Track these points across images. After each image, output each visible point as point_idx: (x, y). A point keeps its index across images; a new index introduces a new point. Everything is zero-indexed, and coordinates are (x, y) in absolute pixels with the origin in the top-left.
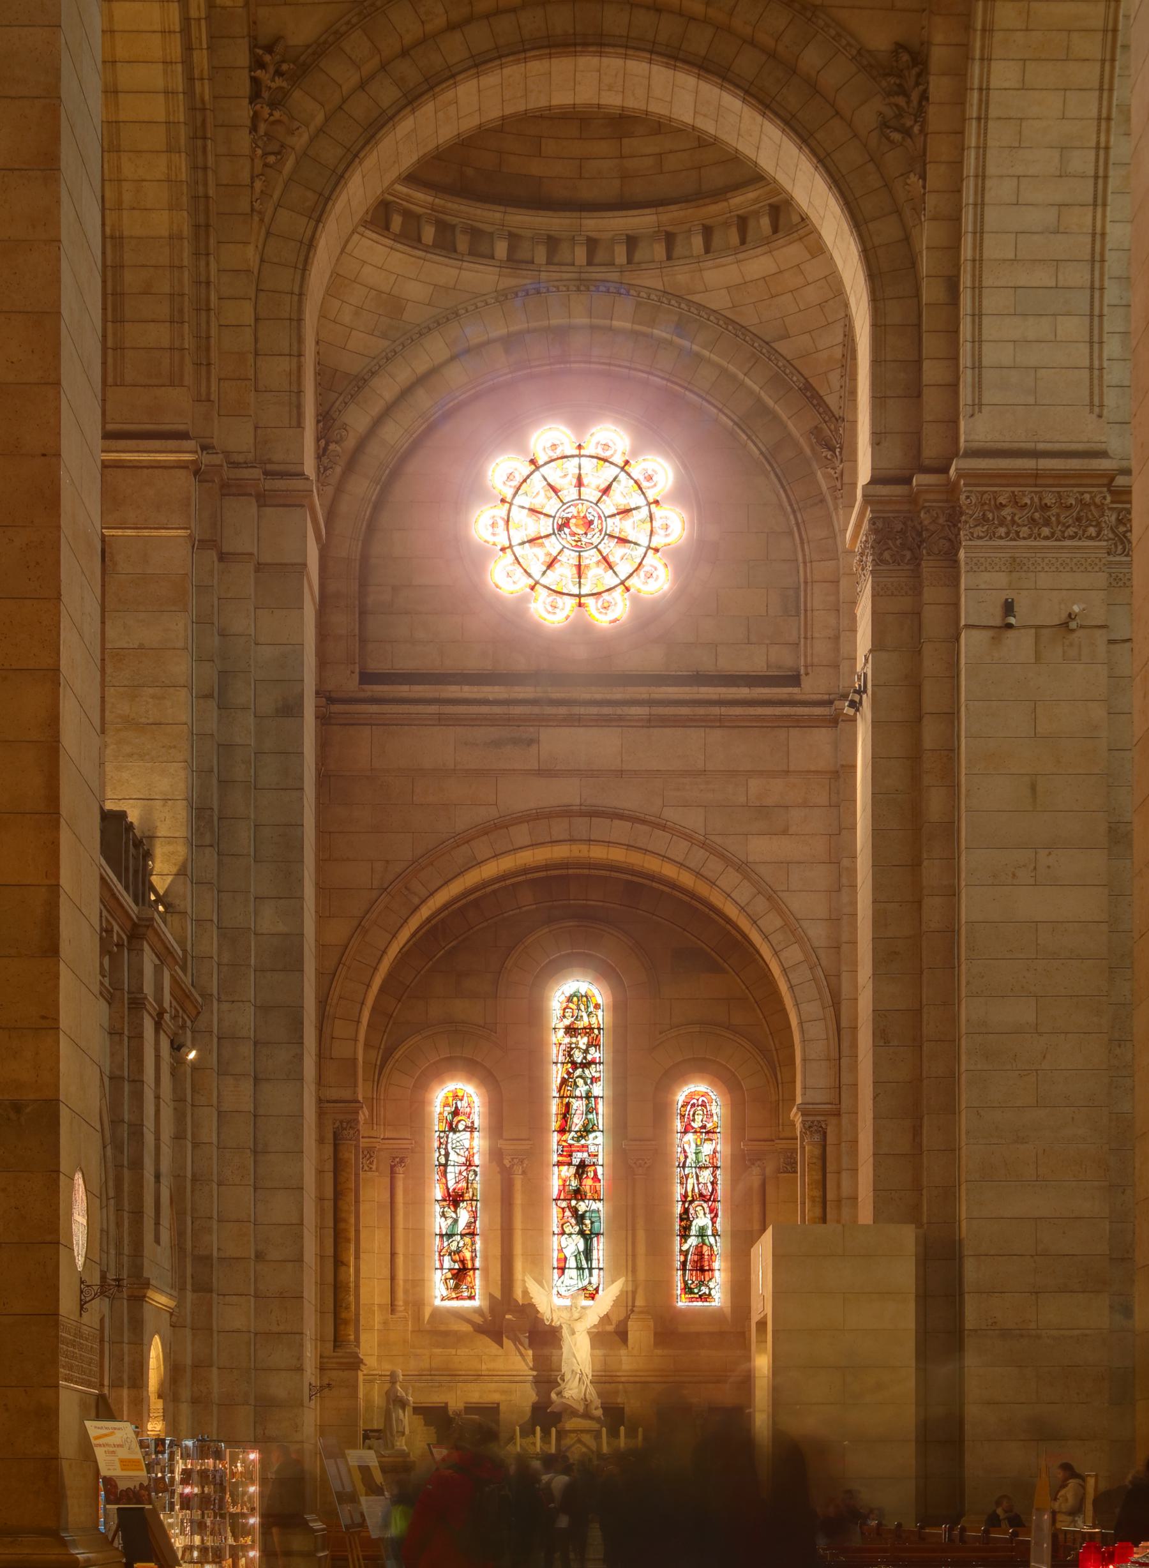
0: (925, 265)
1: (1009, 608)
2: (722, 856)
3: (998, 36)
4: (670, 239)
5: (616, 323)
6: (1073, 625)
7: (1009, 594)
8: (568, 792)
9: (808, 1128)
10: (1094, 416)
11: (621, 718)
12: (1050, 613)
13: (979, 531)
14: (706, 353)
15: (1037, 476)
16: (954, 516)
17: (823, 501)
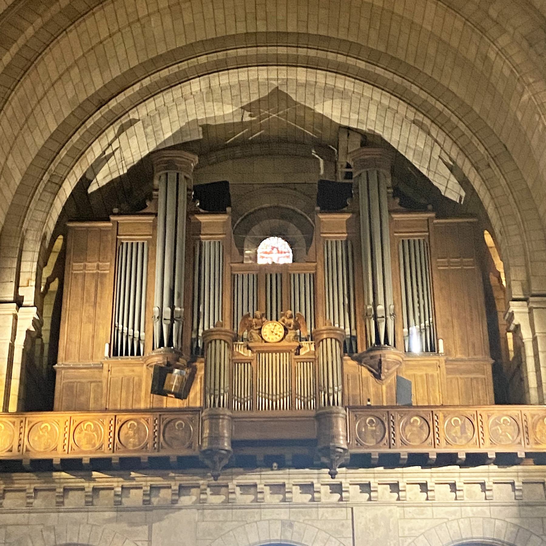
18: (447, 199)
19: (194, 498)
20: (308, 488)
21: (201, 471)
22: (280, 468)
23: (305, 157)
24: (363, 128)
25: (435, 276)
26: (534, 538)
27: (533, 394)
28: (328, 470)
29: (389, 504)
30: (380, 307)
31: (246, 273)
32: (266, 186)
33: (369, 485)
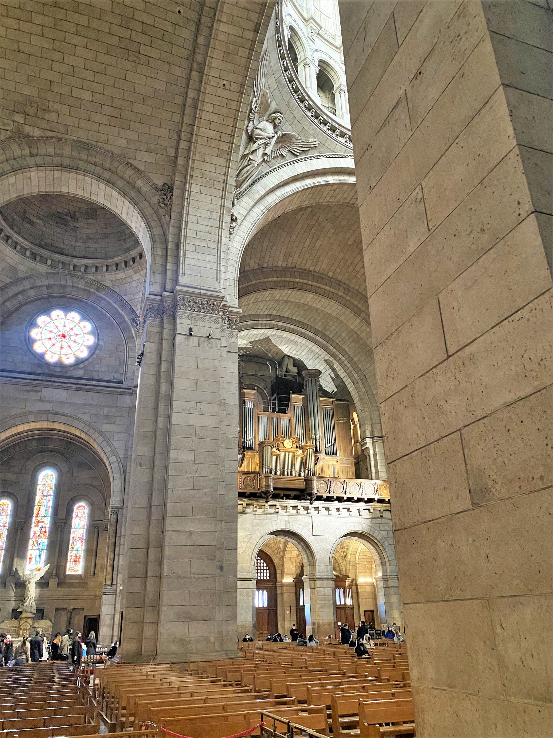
0: (170, 238)
1: (191, 330)
2: (94, 429)
3: (194, 178)
4: (97, 268)
5: (80, 286)
6: (210, 337)
7: (191, 326)
8: (49, 407)
9: (113, 513)
10: (217, 283)
11: (68, 387)
12: (204, 332)
13: (182, 307)
14: (104, 297)
15: (201, 295)
16: (175, 306)
17: (133, 337)
18: (326, 391)
19: (251, 510)
20: (295, 508)
21: (256, 498)
22: (287, 499)
23: (264, 364)
24: (296, 357)
25: (336, 425)
26: (376, 531)
27: (374, 475)
28: (309, 501)
29: (326, 516)
30: (318, 436)
31: (263, 416)
32: (248, 375)
33: (318, 508)
